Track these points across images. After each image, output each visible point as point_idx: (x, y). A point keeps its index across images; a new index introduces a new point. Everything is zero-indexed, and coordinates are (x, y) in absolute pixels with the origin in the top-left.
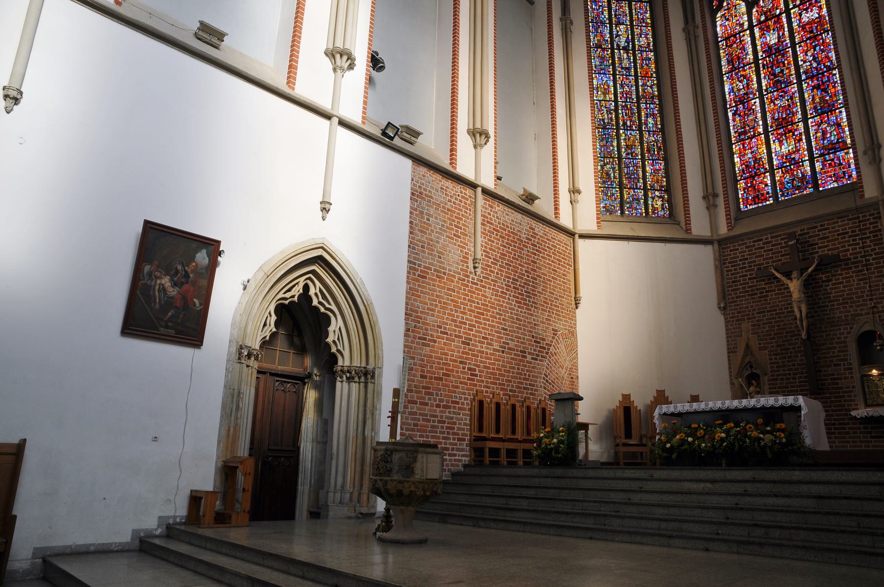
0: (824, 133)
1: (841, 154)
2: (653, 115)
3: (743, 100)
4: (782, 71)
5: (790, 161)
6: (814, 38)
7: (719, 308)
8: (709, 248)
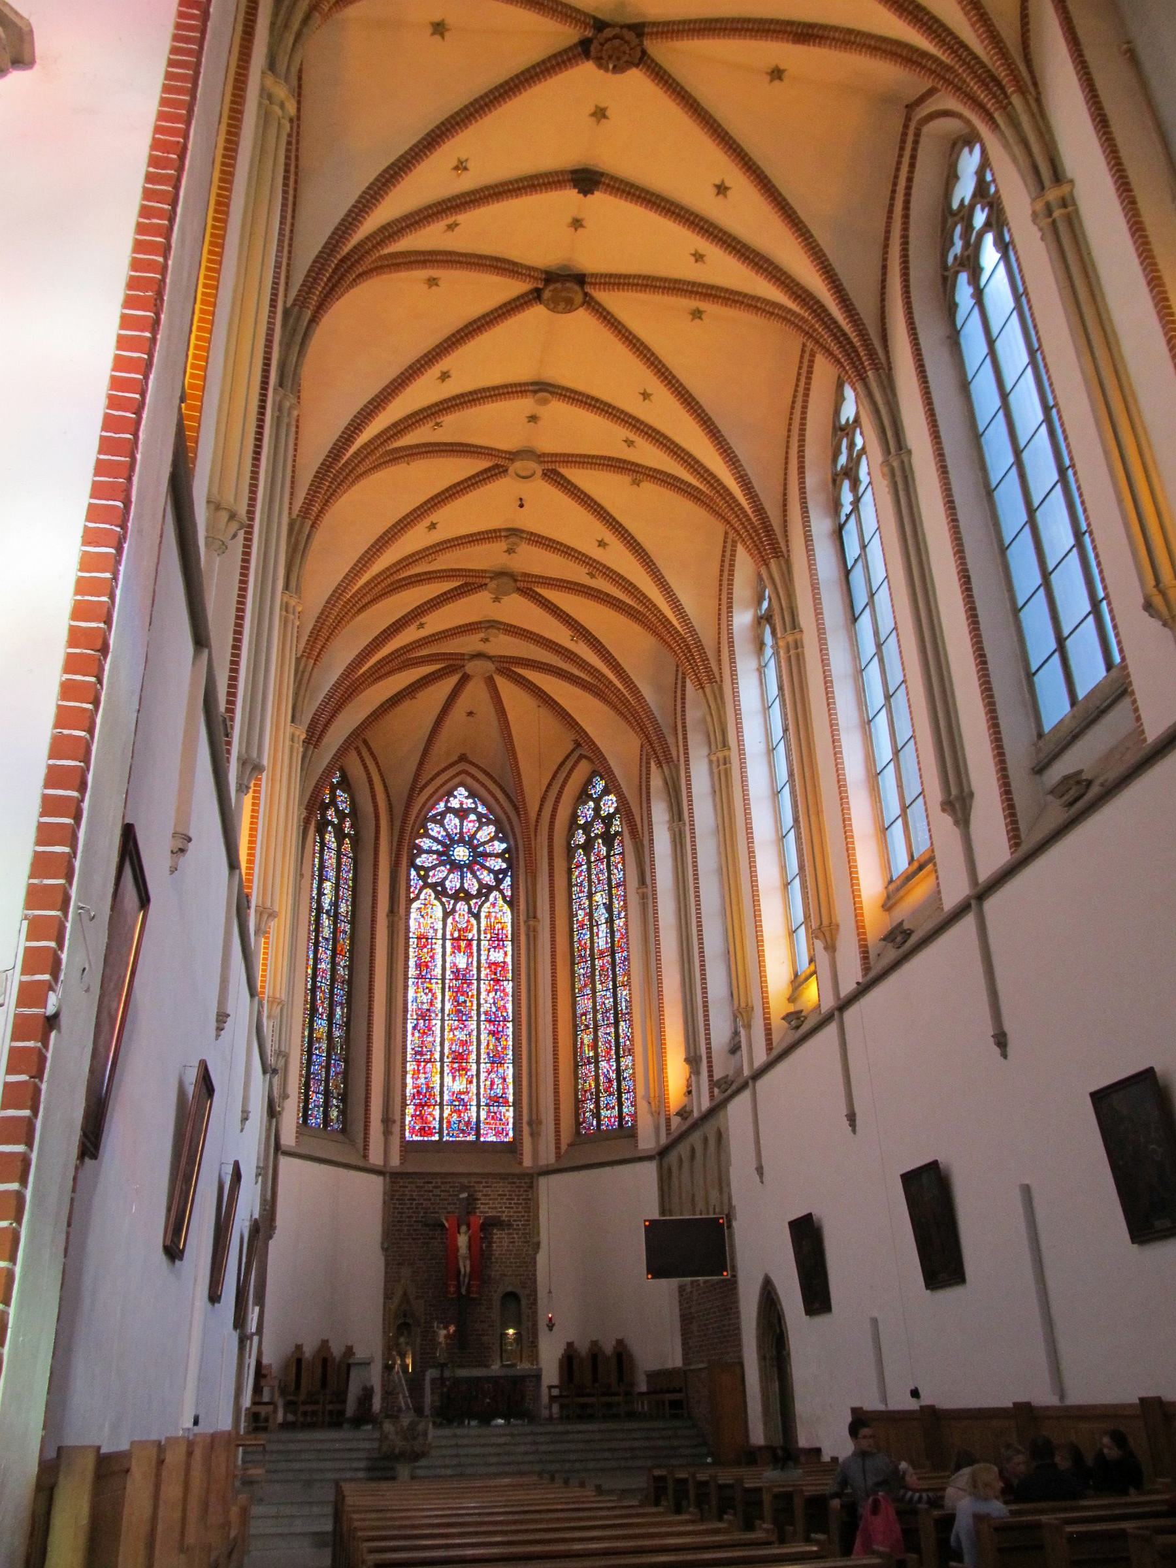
0: (492, 1083)
1: (503, 1109)
2: (341, 1004)
3: (424, 1015)
4: (465, 1002)
5: (460, 1102)
6: (497, 981)
7: (382, 1248)
8: (381, 1178)
